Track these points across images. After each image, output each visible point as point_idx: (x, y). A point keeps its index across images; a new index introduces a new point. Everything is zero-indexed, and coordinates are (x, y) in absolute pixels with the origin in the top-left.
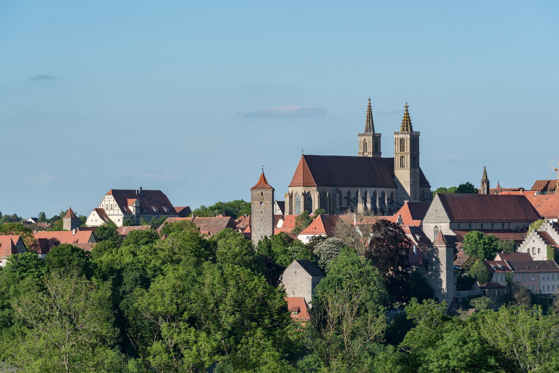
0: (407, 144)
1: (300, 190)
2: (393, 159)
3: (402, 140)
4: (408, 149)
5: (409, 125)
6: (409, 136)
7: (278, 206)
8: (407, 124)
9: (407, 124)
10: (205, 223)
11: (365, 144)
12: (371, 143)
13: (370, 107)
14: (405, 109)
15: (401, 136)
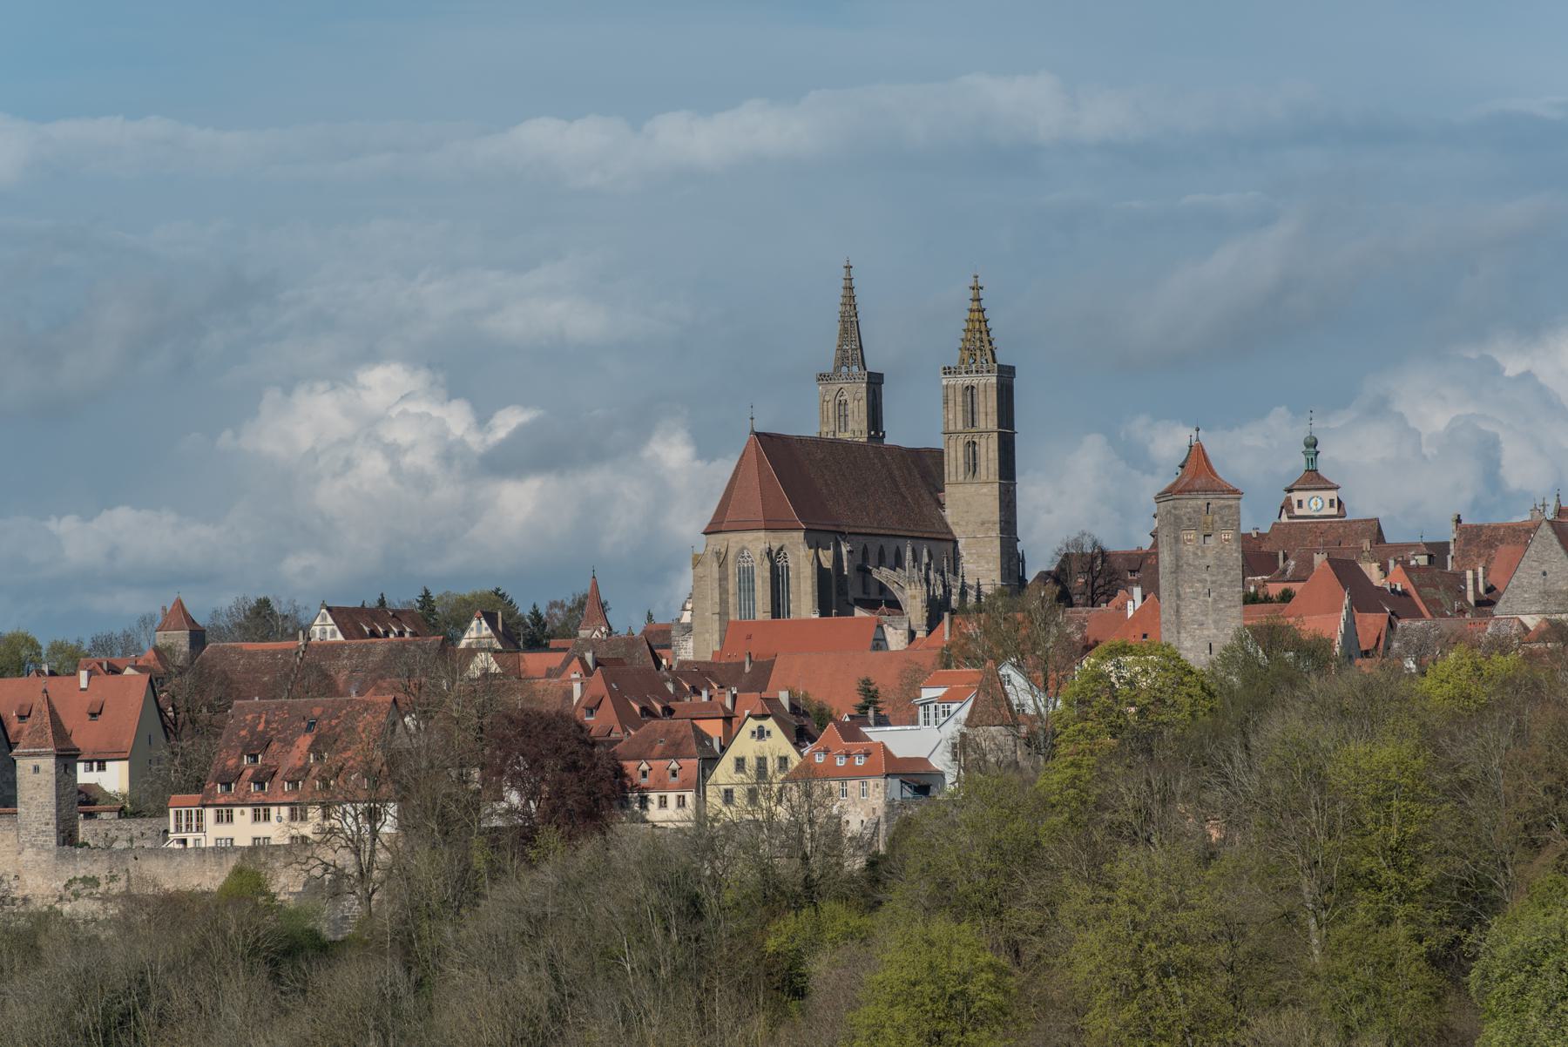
0: (988, 406)
1: (756, 543)
2: (941, 452)
3: (970, 389)
4: (988, 418)
5: (987, 347)
6: (994, 380)
7: (330, 620)
8: (979, 338)
9: (979, 338)
10: (350, 657)
11: (842, 404)
12: (863, 403)
13: (851, 289)
14: (971, 294)
15: (967, 380)
